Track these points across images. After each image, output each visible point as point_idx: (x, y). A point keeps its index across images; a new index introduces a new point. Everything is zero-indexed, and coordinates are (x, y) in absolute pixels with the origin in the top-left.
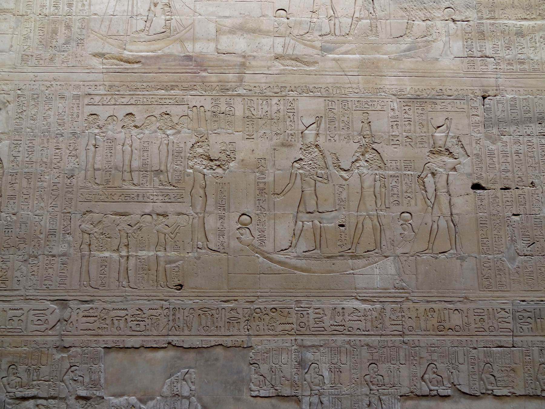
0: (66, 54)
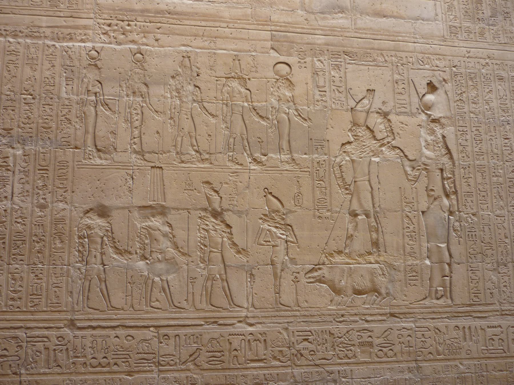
0: (495, 28)
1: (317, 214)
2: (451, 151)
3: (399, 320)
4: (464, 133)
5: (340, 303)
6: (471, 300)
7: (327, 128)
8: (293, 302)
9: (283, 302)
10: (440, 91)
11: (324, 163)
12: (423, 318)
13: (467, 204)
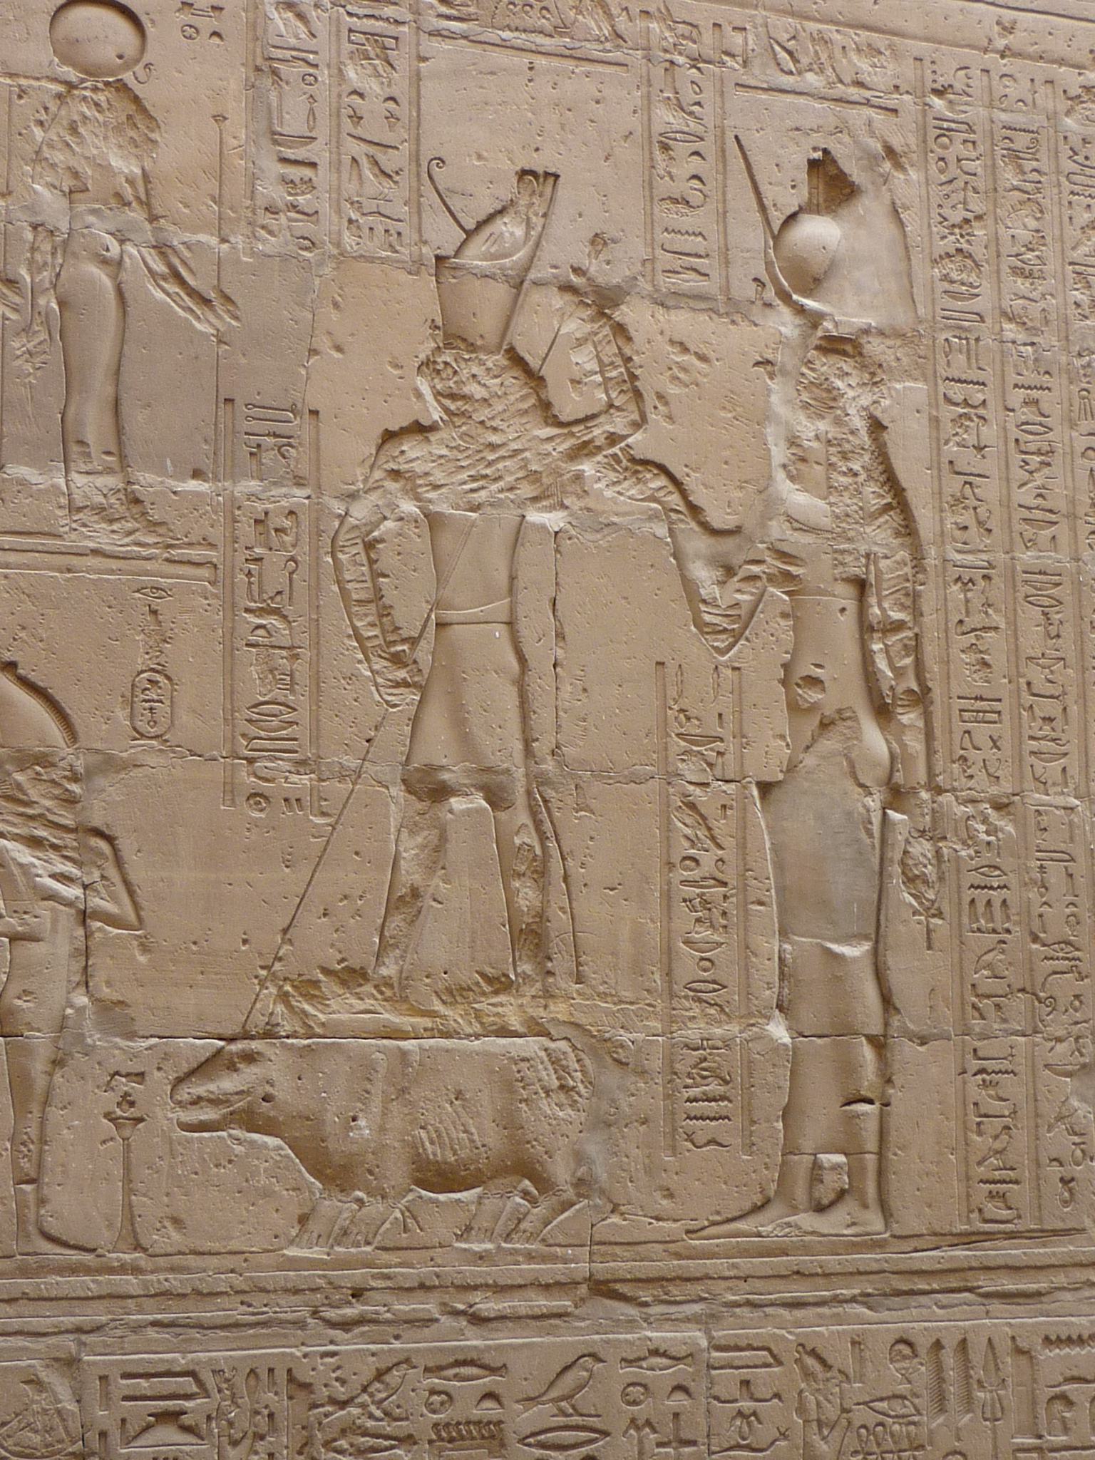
1: (246, 779)
2: (910, 495)
3: (633, 1311)
4: (971, 412)
5: (345, 1233)
6: (975, 1215)
7: (313, 352)
8: (110, 1226)
9: (54, 1227)
10: (870, 206)
11: (287, 523)
12: (749, 1303)
13: (972, 754)
